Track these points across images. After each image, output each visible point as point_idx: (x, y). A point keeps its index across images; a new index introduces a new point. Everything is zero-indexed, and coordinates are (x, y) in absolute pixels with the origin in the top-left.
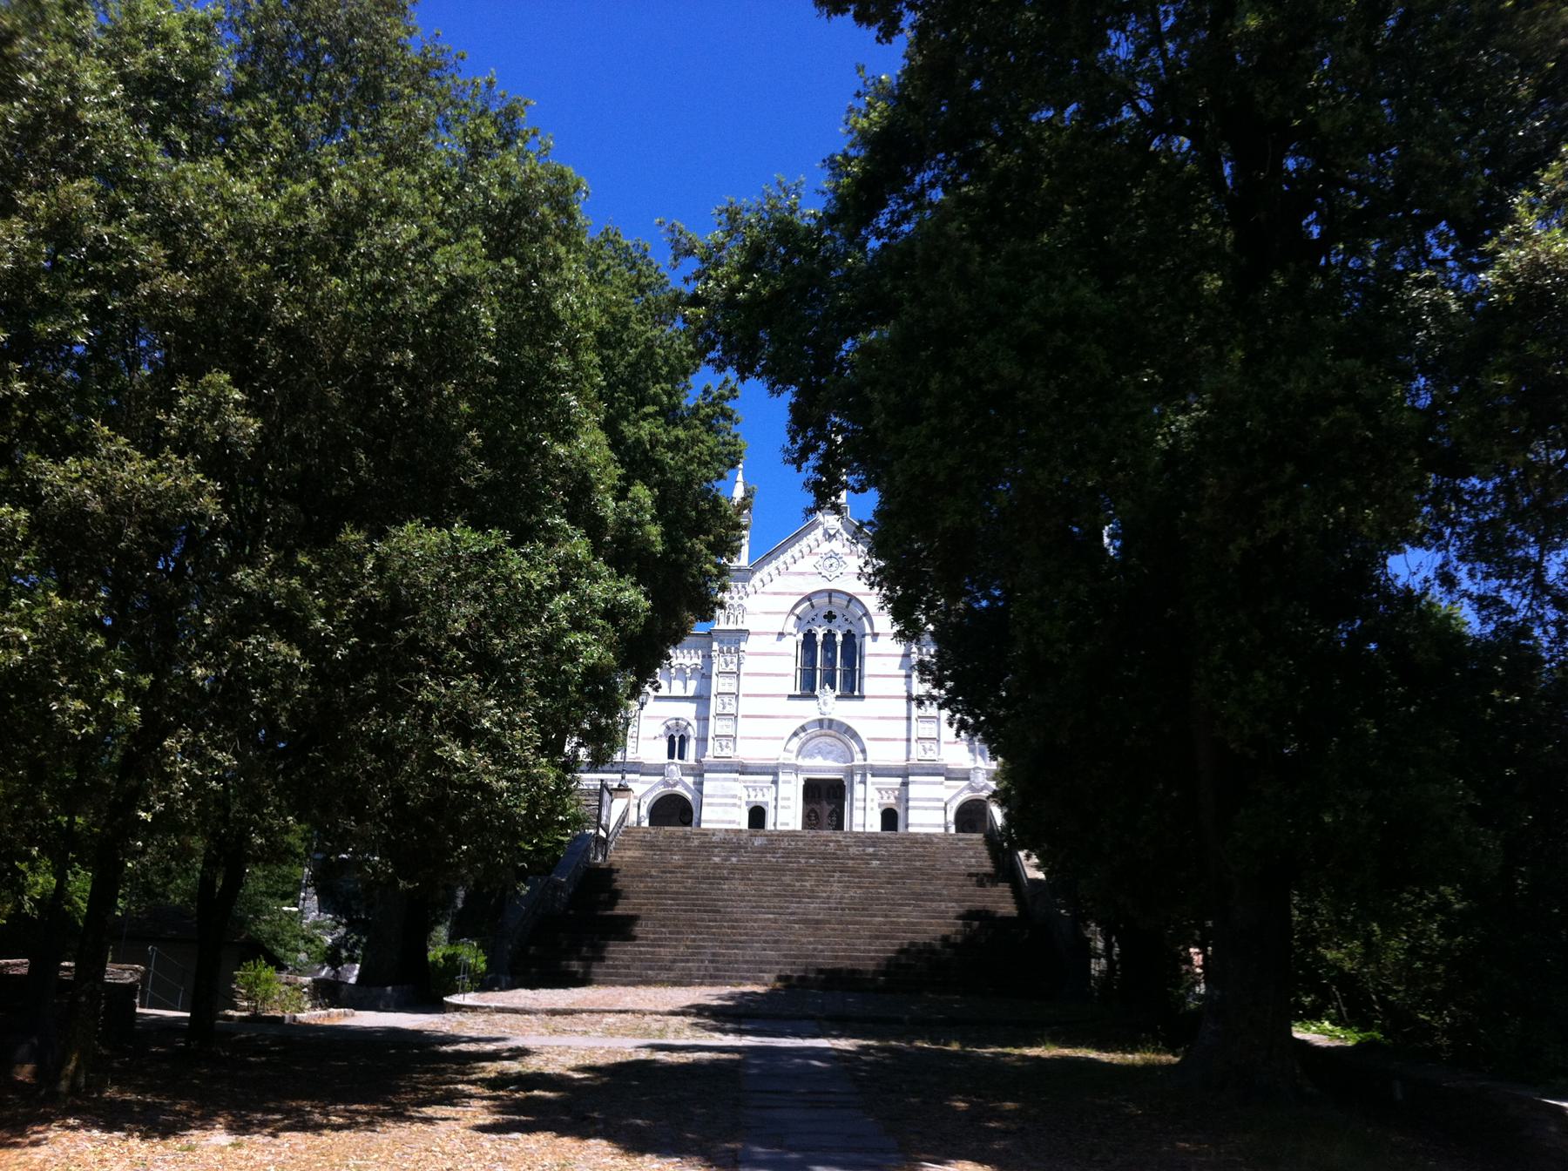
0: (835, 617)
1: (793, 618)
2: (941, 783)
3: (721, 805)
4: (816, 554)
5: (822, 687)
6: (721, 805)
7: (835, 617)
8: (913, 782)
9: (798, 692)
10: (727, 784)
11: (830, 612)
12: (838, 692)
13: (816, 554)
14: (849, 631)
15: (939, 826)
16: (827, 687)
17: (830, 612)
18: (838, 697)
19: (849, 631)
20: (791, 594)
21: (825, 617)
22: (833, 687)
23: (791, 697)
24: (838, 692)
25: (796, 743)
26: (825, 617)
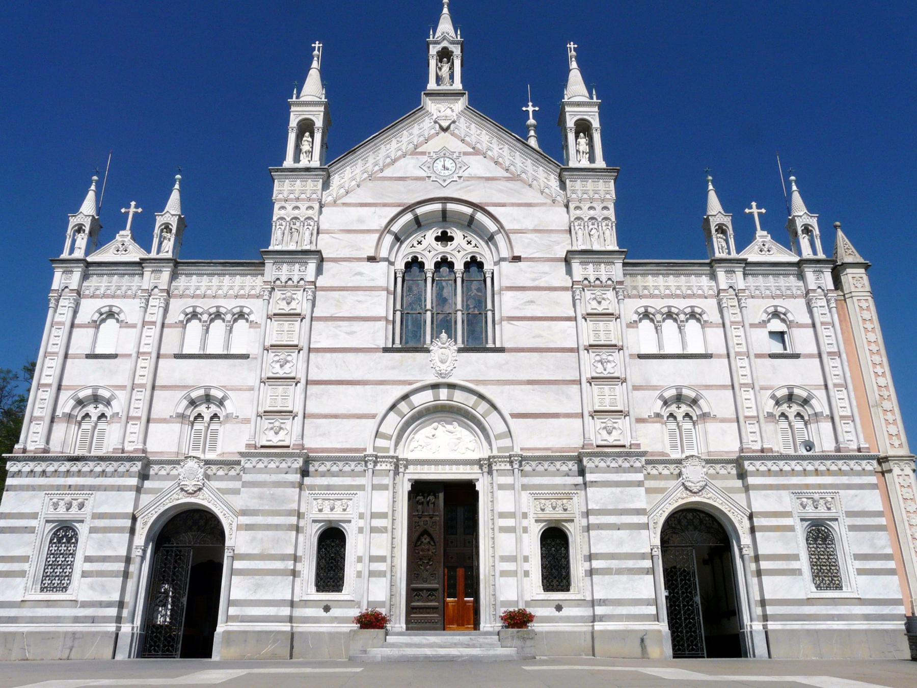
0: (451, 239)
1: (389, 239)
2: (640, 484)
3: (268, 527)
4: (423, 153)
5: (435, 335)
6: (268, 527)
7: (451, 239)
8: (594, 483)
9: (398, 345)
10: (279, 491)
11: (444, 233)
12: (460, 344)
13: (423, 153)
14: (473, 258)
15: (643, 556)
16: (444, 335)
17: (444, 233)
18: (460, 350)
19: (473, 258)
20: (385, 205)
21: (437, 239)
22: (451, 335)
23: (386, 350)
24: (460, 344)
25: (392, 423)
26: (437, 239)
